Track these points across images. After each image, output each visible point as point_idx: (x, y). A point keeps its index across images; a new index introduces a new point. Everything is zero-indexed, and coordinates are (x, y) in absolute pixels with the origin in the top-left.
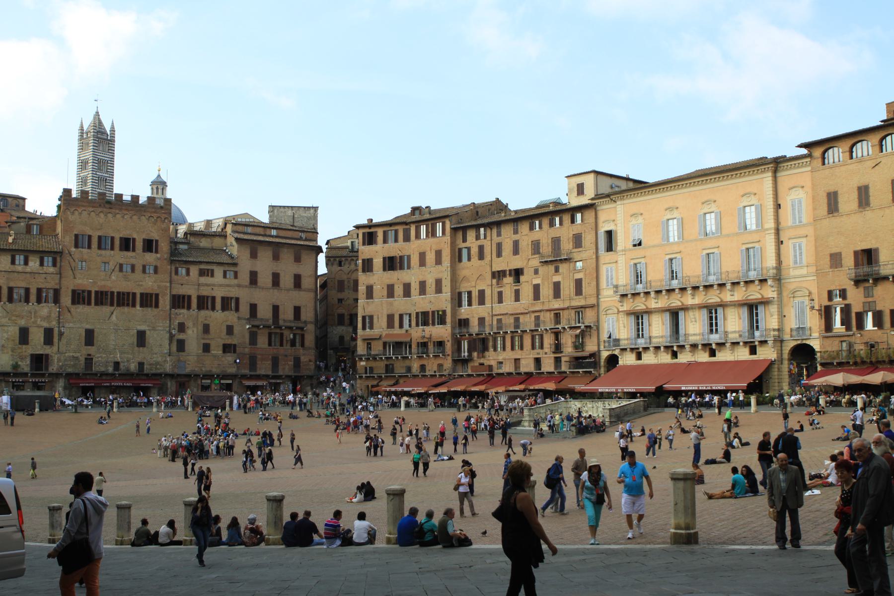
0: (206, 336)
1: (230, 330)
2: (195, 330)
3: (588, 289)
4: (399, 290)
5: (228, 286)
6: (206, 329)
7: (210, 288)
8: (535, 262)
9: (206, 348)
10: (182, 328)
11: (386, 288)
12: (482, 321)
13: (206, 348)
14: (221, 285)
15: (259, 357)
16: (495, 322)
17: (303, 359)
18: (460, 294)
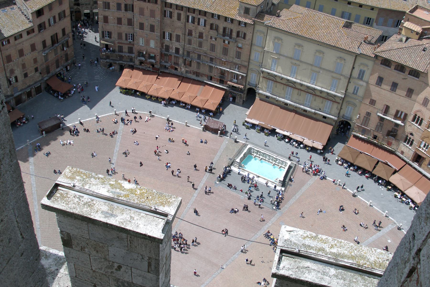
0: (25, 70)
1: (35, 61)
2: (19, 69)
3: (244, 57)
4: (125, 21)
5: (31, 38)
6: (24, 66)
7: (22, 44)
8: (213, 33)
9: (26, 75)
10: (12, 71)
11: (116, 19)
12: (177, 50)
13: (26, 75)
14: (27, 40)
15: (50, 65)
16: (185, 53)
17: (69, 53)
18: (164, 33)
